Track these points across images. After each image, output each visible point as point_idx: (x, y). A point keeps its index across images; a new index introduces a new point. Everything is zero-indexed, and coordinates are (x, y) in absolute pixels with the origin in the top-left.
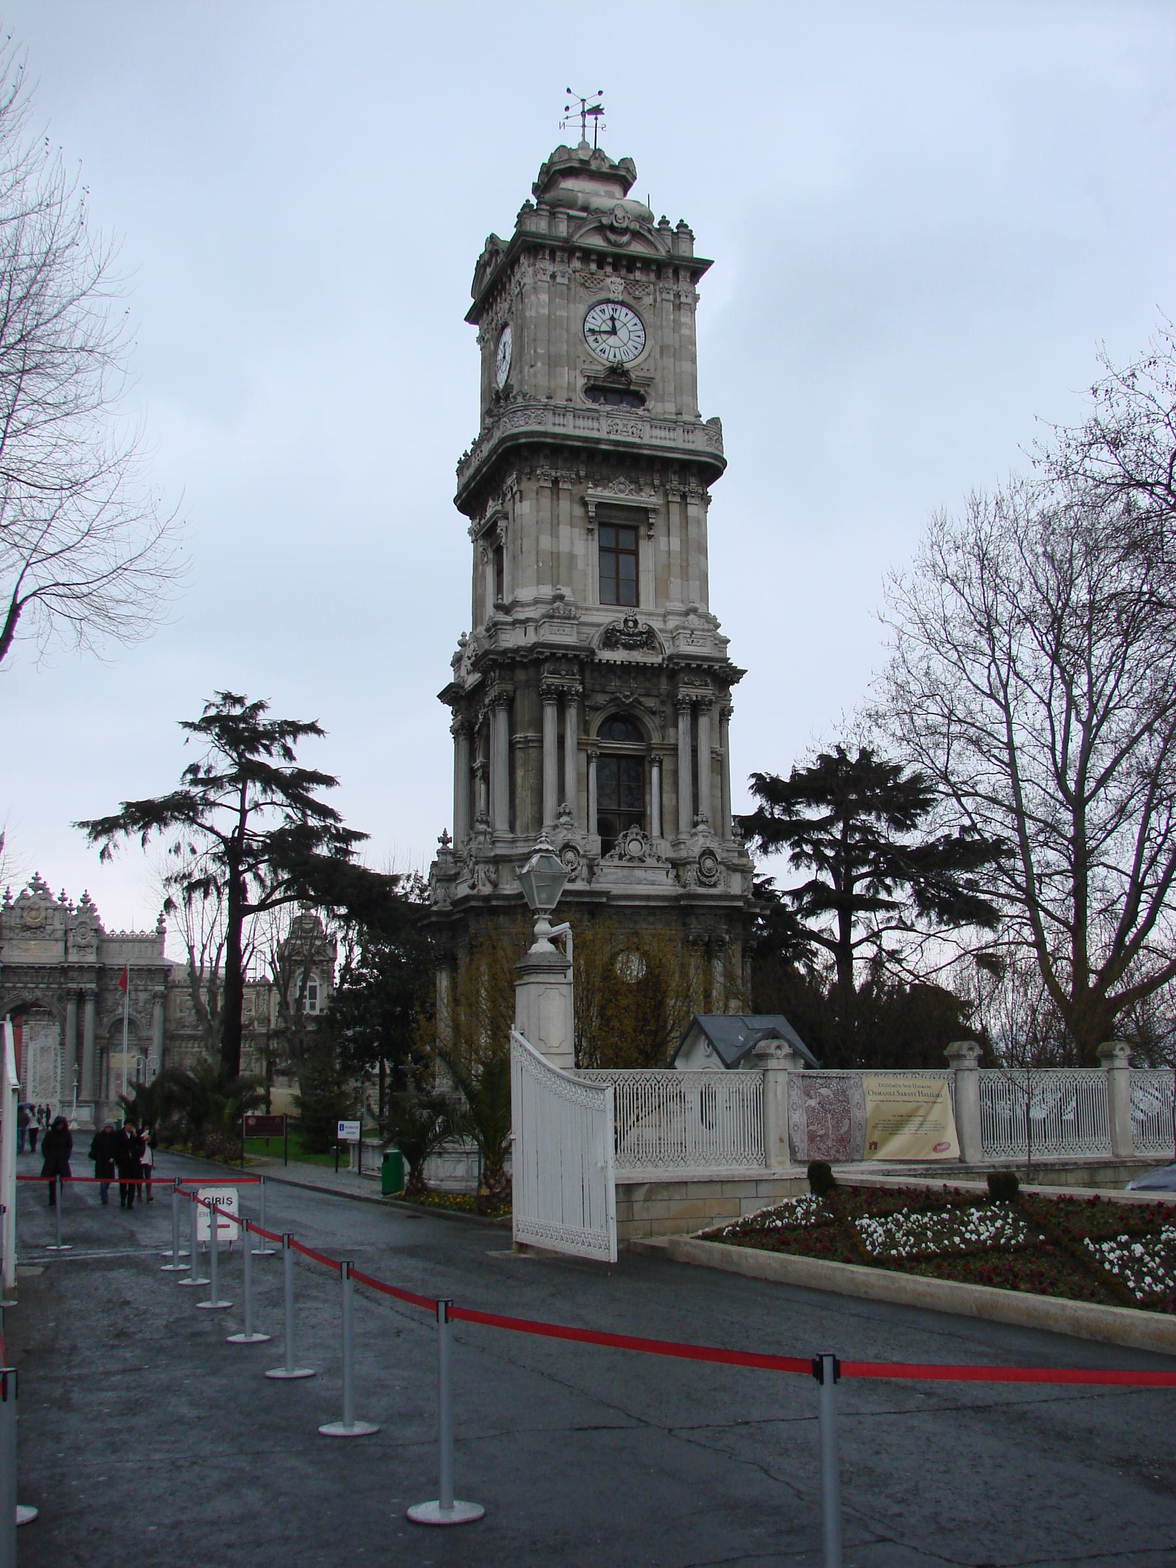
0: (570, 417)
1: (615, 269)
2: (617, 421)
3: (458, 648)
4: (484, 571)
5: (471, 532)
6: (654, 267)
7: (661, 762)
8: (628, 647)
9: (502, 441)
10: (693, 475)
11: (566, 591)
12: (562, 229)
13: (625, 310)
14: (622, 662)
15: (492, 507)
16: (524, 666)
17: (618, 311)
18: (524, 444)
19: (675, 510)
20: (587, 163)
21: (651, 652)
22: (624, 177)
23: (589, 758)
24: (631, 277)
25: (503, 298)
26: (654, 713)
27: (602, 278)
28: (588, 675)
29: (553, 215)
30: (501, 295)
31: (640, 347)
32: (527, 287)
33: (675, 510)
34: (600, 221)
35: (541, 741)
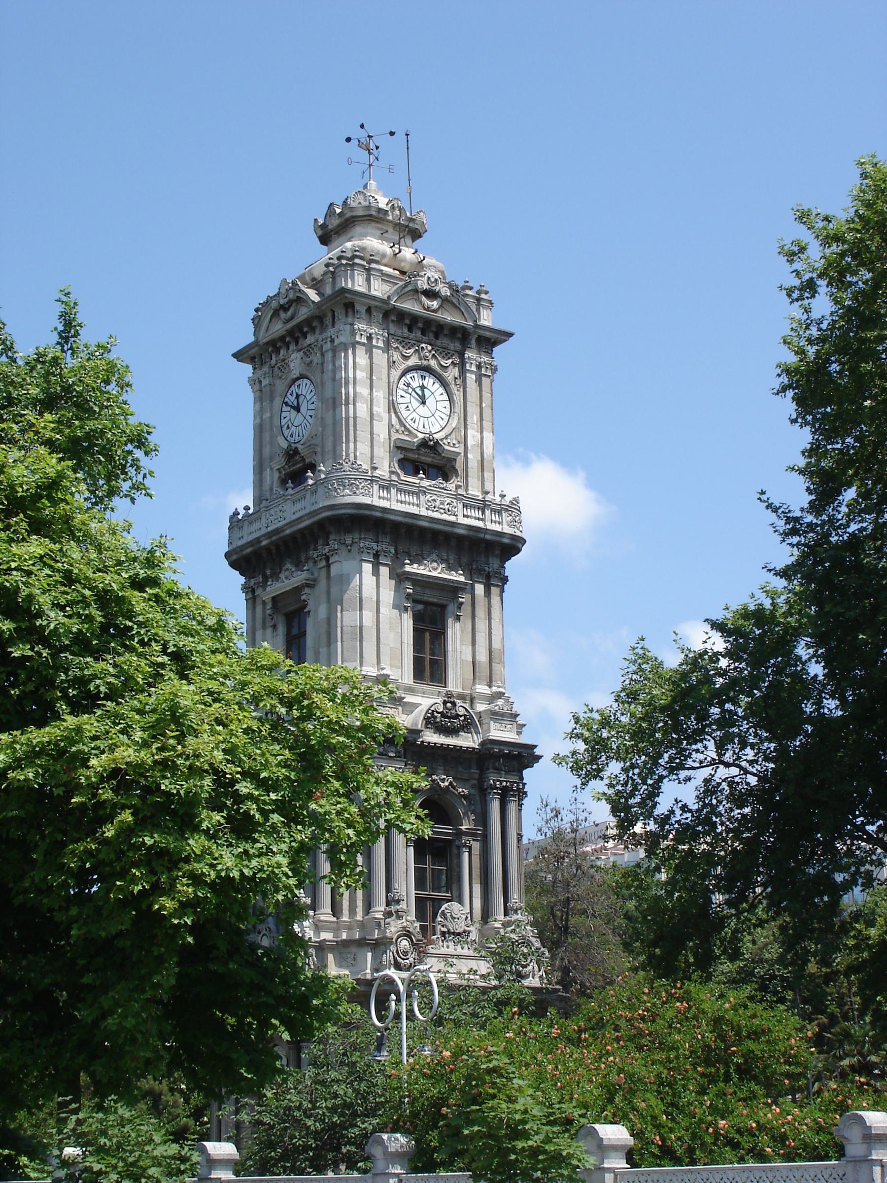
2: (434, 497)
7: (470, 848)
12: (379, 289)
31: (446, 418)
33: (479, 589)
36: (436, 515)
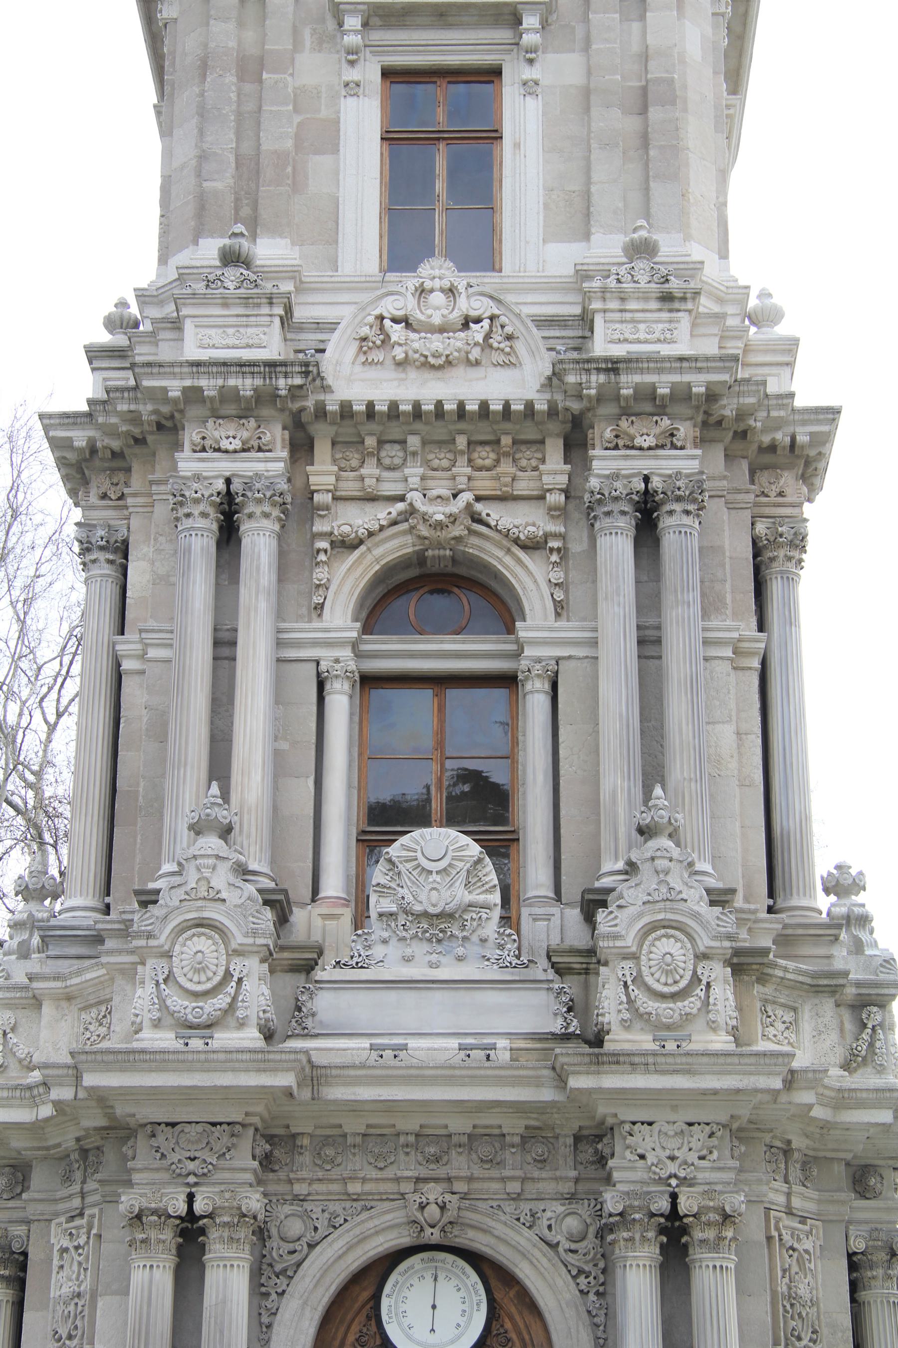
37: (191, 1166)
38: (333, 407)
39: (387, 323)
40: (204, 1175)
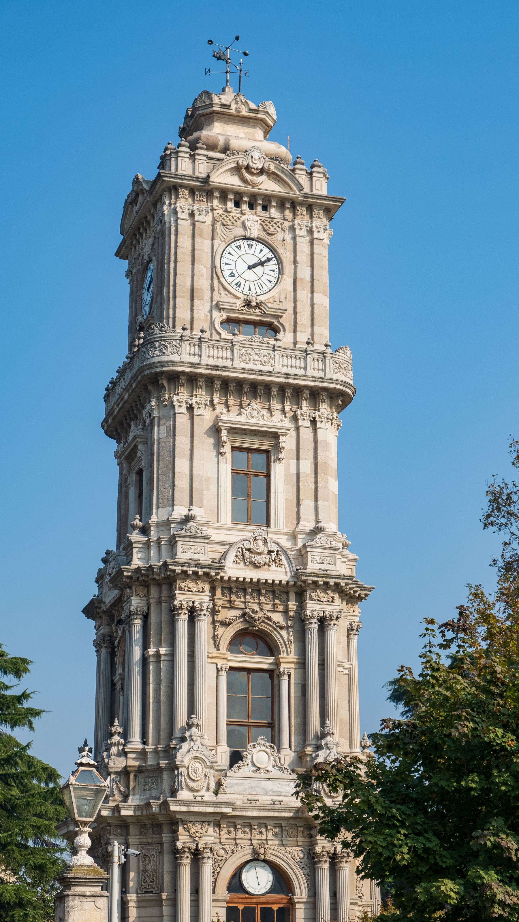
0: (204, 346)
1: (251, 206)
3: (102, 565)
4: (127, 493)
5: (117, 455)
6: (288, 205)
7: (289, 676)
8: (256, 566)
9: (141, 370)
10: (323, 401)
11: (196, 511)
13: (260, 246)
14: (251, 579)
15: (134, 431)
16: (159, 584)
17: (254, 247)
18: (163, 372)
19: (306, 434)
20: (228, 106)
21: (279, 569)
22: (262, 120)
23: (218, 670)
24: (266, 214)
25: (148, 235)
26: (281, 628)
27: (239, 215)
28: (218, 592)
29: (193, 157)
30: (146, 232)
31: (274, 281)
32: (167, 225)
33: (306, 434)
34: (237, 162)
35: (172, 656)
36: (251, 366)
37: (197, 834)
38: (226, 578)
39: (244, 550)
40: (201, 837)
